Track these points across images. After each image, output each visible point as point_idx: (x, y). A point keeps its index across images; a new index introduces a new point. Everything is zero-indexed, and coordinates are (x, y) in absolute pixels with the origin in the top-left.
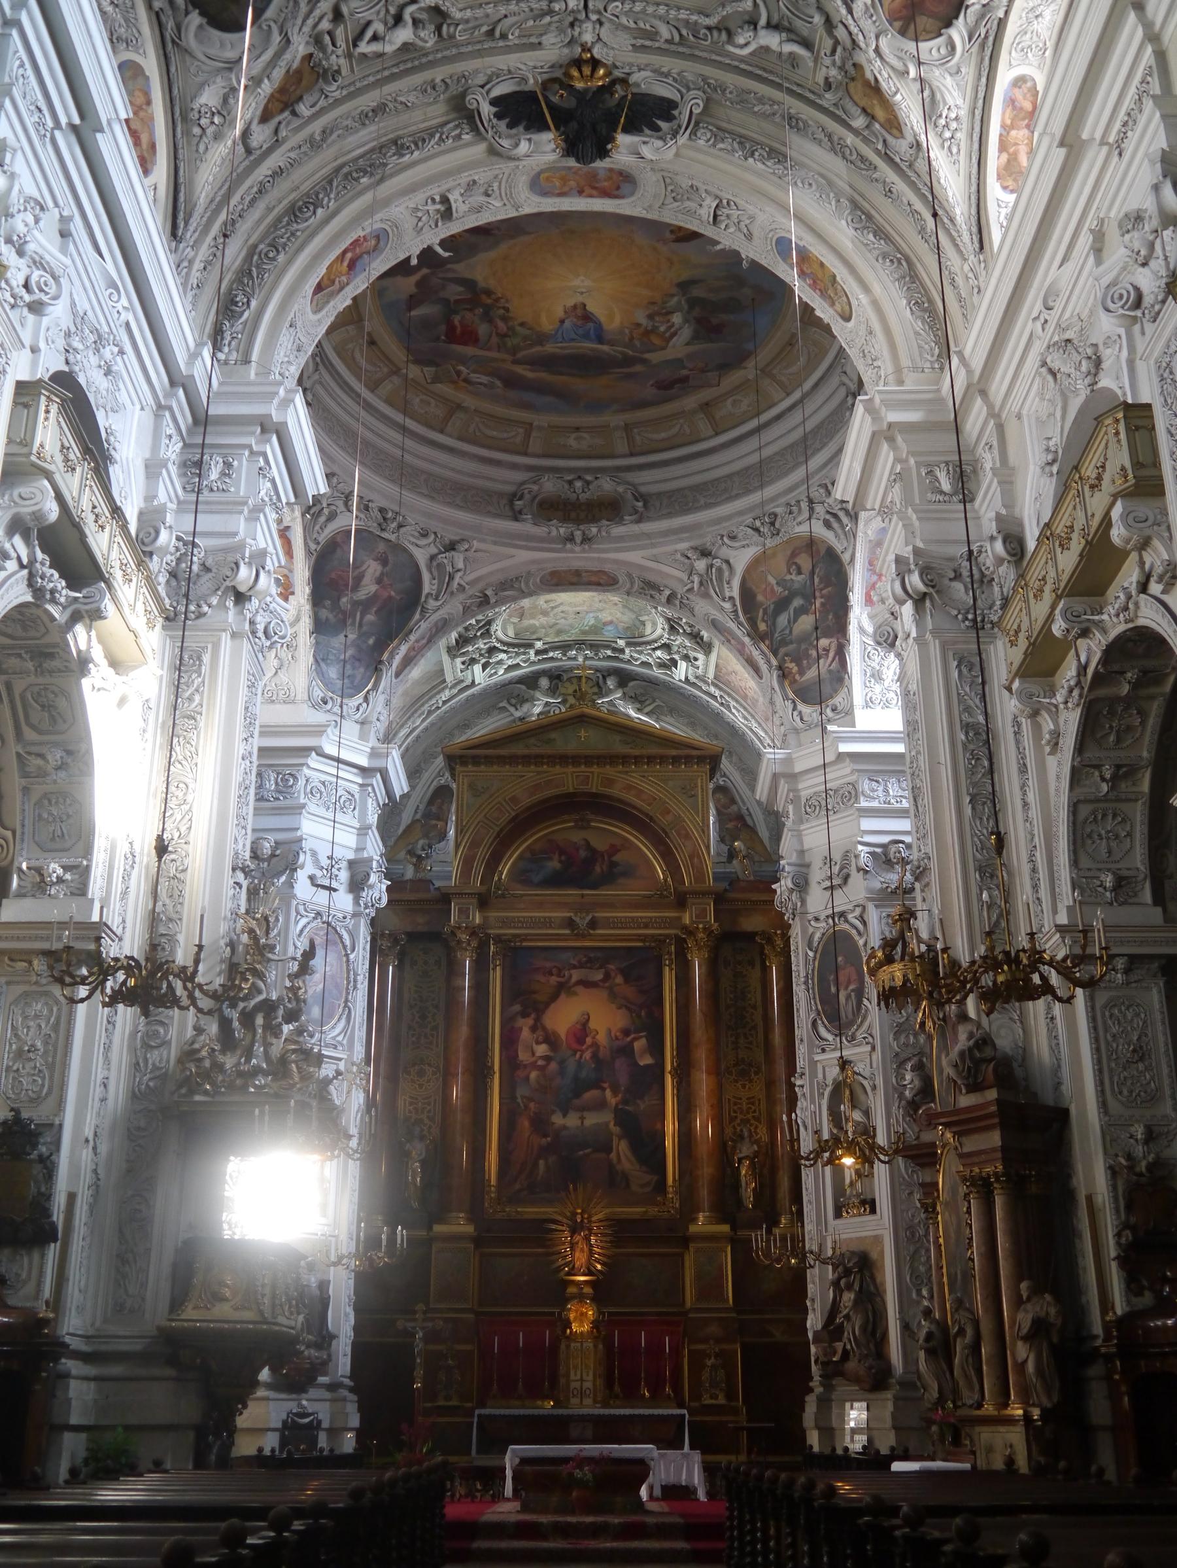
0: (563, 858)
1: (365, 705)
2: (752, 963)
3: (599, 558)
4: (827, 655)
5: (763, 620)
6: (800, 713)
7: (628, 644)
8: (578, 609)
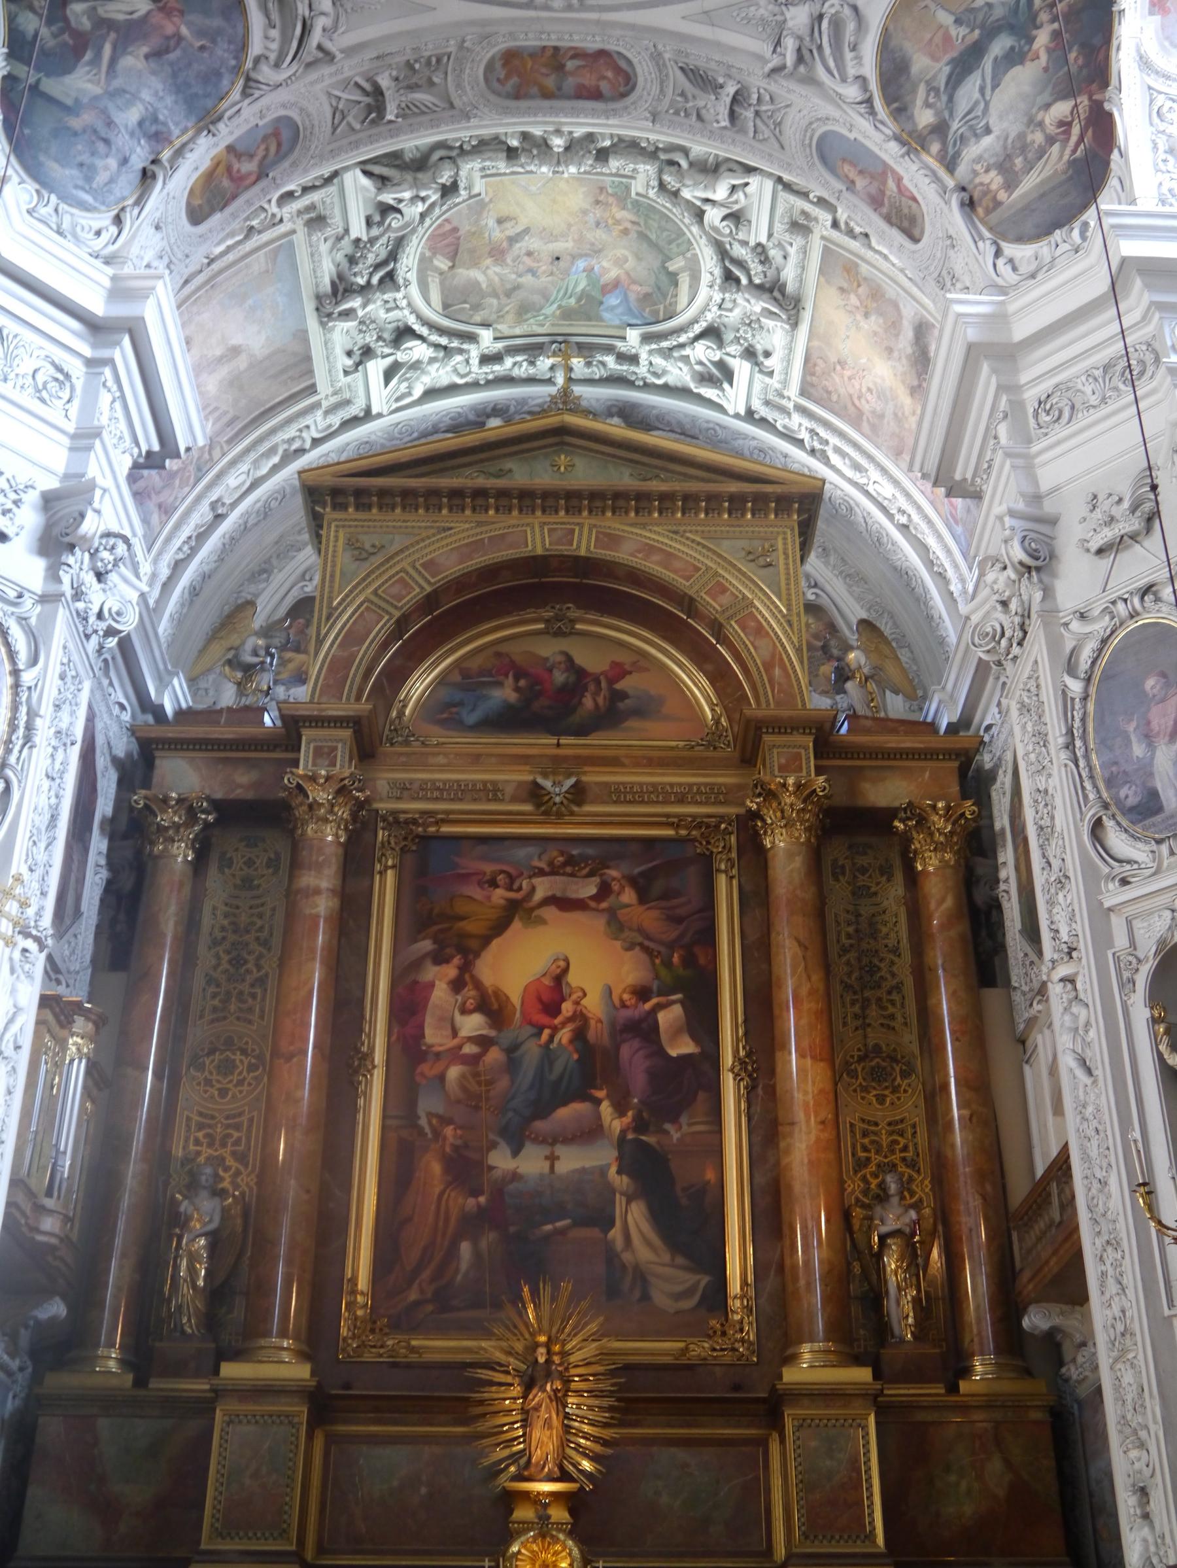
0: (522, 683)
1: (114, 230)
2: (886, 871)
3: (598, 22)
4: (1068, 133)
5: (928, 105)
6: (1011, 261)
7: (647, 338)
8: (559, 246)
